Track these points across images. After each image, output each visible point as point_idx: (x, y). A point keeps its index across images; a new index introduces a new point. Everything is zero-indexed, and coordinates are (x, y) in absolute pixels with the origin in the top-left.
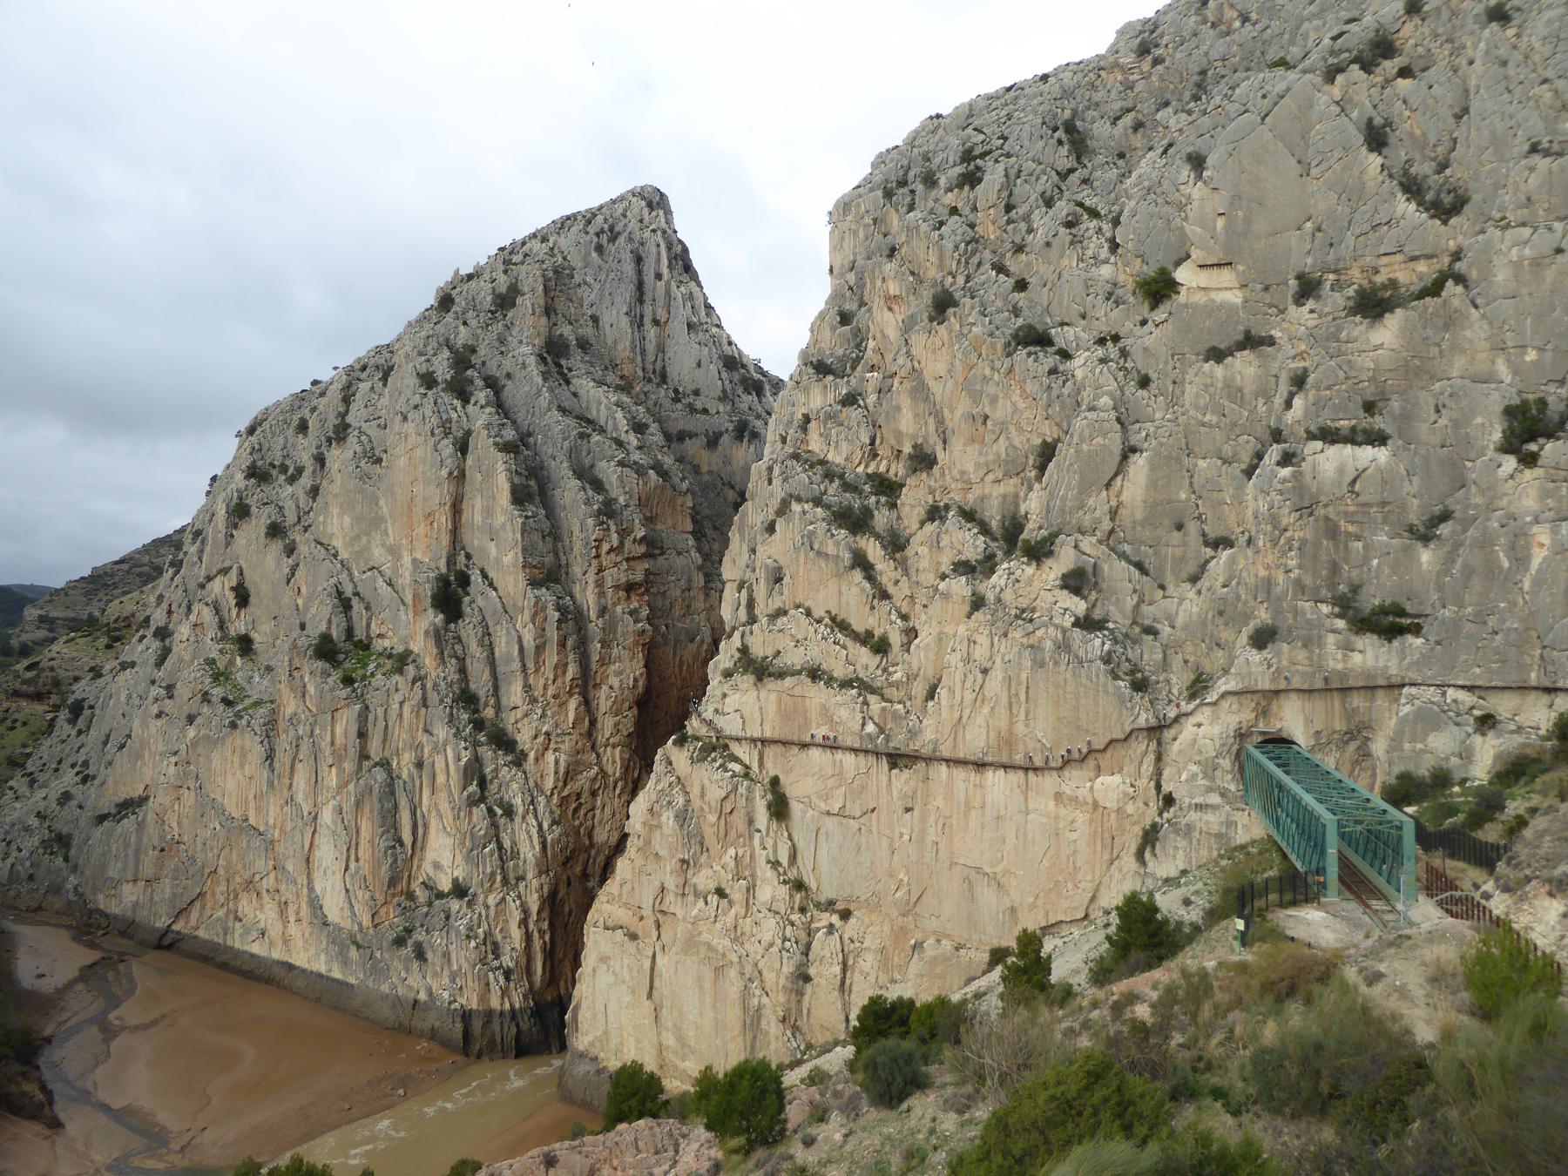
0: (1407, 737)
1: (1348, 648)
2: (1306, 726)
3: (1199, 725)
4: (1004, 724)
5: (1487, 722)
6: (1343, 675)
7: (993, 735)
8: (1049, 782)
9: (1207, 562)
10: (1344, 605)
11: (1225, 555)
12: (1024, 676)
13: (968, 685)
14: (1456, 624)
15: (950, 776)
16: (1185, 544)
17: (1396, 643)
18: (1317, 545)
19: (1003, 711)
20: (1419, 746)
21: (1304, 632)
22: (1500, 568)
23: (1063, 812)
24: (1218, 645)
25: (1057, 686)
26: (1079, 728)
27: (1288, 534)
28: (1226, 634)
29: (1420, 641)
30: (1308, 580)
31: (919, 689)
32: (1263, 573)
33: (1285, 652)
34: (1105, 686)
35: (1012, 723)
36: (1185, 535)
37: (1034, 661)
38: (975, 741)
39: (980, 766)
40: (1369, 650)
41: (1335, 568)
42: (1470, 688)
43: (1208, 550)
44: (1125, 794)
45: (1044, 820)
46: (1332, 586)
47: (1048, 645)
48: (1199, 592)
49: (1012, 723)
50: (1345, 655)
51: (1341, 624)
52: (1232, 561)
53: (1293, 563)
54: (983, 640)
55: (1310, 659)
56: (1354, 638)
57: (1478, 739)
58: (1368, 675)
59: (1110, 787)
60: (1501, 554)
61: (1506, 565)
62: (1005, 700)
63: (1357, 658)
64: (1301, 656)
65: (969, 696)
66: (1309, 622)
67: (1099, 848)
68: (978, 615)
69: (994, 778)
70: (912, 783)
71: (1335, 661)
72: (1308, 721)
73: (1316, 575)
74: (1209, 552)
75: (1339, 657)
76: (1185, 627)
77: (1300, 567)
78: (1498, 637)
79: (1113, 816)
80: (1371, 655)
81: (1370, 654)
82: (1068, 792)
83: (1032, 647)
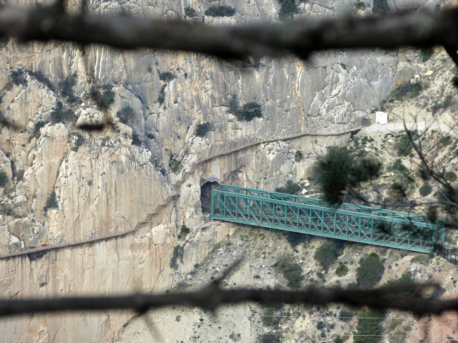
0: (274, 170)
1: (236, 128)
2: (221, 172)
3: (190, 186)
4: (104, 213)
5: (299, 156)
6: (235, 144)
7: (97, 221)
8: (127, 241)
9: (163, 88)
10: (233, 107)
11: (172, 83)
12: (113, 181)
13: (81, 194)
14: (273, 108)
15: (73, 255)
16: (152, 80)
17: (252, 122)
18: (217, 75)
19: (103, 206)
20: (278, 172)
21: (219, 124)
22: (285, 79)
23: (136, 254)
24: (179, 137)
25: (131, 182)
26: (142, 203)
27: (204, 70)
28: (181, 130)
29: (262, 119)
30: (216, 95)
31: (38, 204)
32: (195, 93)
33: (214, 136)
34: (154, 176)
35: (108, 211)
36: (153, 74)
37: (118, 170)
38: (86, 231)
39: (91, 243)
40: (243, 127)
41: (225, 87)
42: (285, 140)
43: (162, 81)
44: (166, 233)
45: (128, 262)
46: (226, 98)
47: (123, 159)
48: (165, 108)
49: (108, 211)
50: (235, 132)
51: (231, 116)
52: (175, 87)
53: (209, 86)
54: (86, 163)
55: (222, 137)
56: (238, 123)
57: (297, 164)
58: (244, 141)
59: (159, 231)
60: (285, 72)
61: (287, 77)
62: (104, 198)
63: (239, 132)
64: (219, 136)
65: (82, 202)
66: (219, 117)
67: (154, 268)
68: (82, 149)
69: (100, 248)
70: (45, 268)
71: (231, 135)
72: (222, 170)
73: (219, 92)
74: (162, 83)
75: (233, 134)
76: (164, 130)
77: (213, 88)
78: (289, 113)
79: (161, 248)
80: (246, 130)
81: (244, 130)
82: (137, 242)
83: (114, 162)
